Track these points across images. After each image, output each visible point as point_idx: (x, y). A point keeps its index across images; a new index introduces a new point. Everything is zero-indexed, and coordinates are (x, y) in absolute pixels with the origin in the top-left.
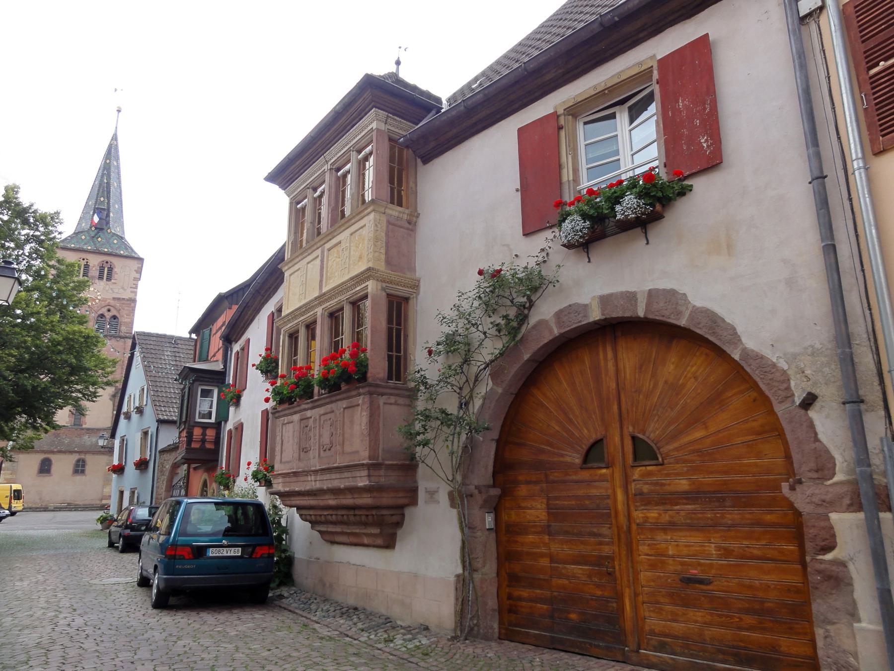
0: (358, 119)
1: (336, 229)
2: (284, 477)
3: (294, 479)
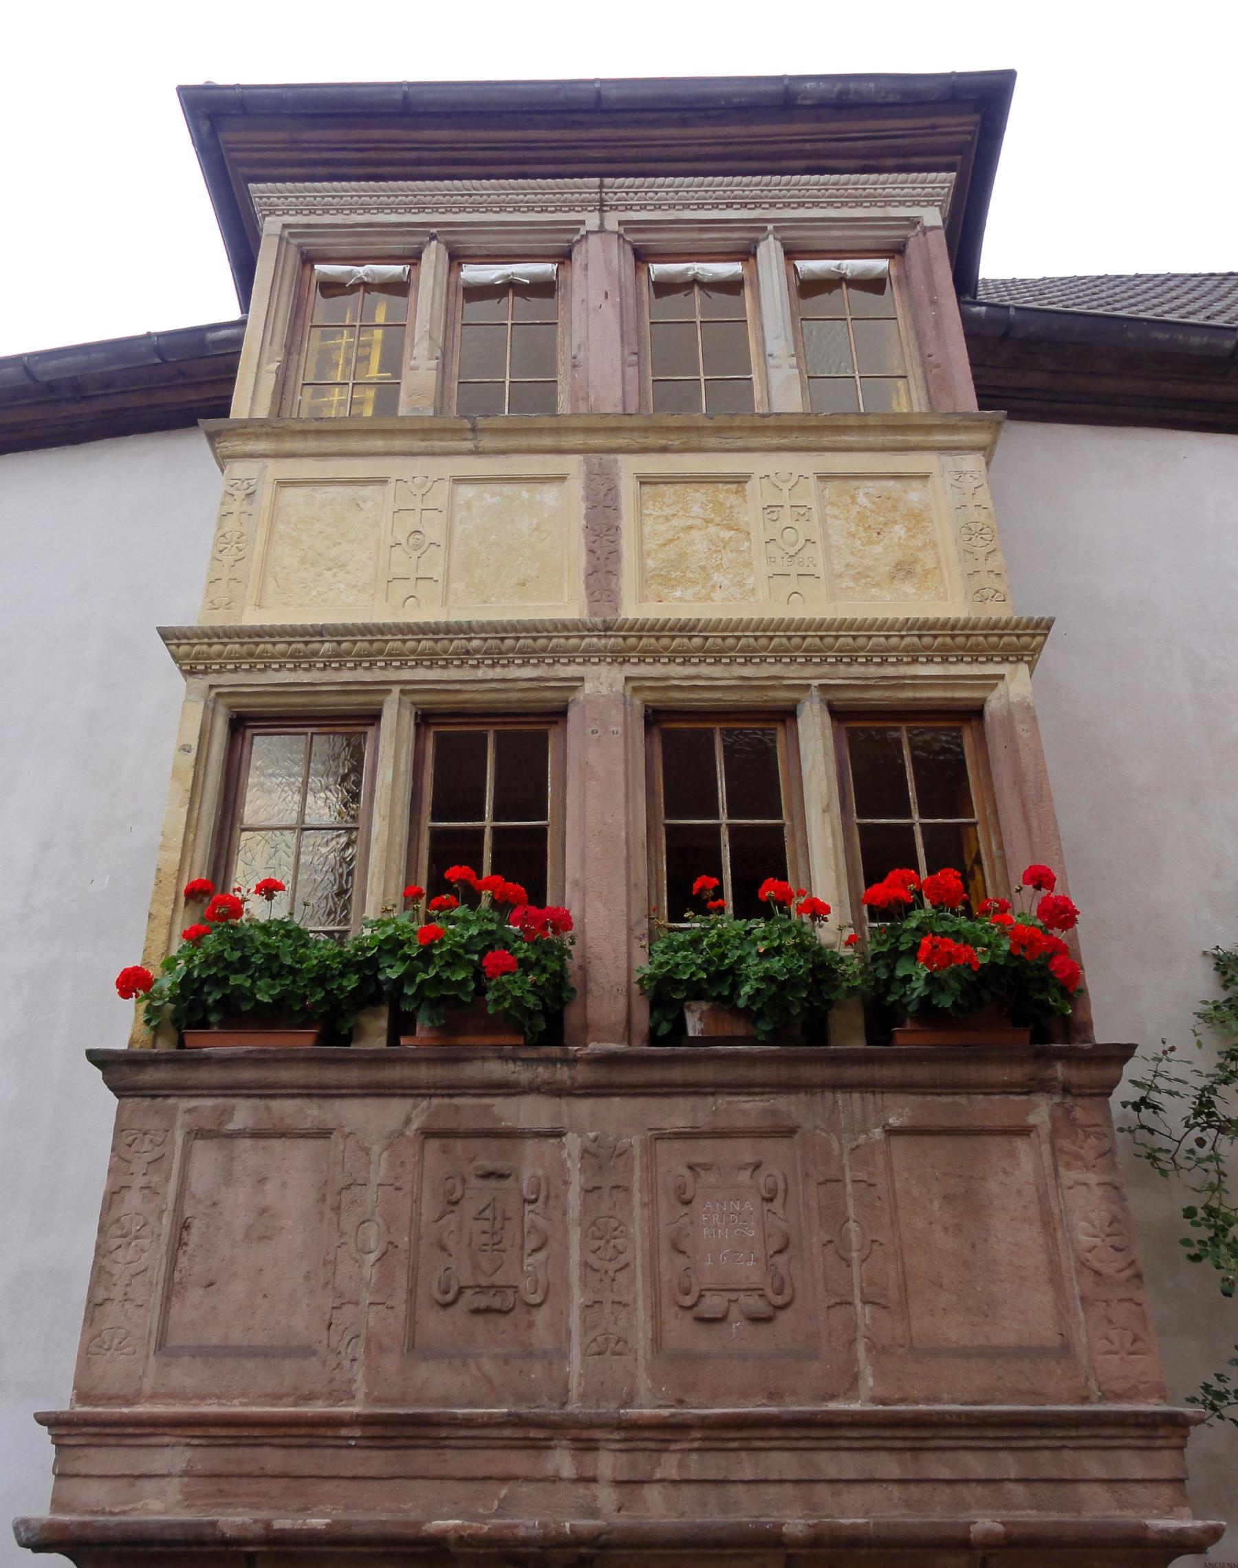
0: (853, 163)
1: (731, 429)
2: (214, 1443)
3: (377, 1461)
